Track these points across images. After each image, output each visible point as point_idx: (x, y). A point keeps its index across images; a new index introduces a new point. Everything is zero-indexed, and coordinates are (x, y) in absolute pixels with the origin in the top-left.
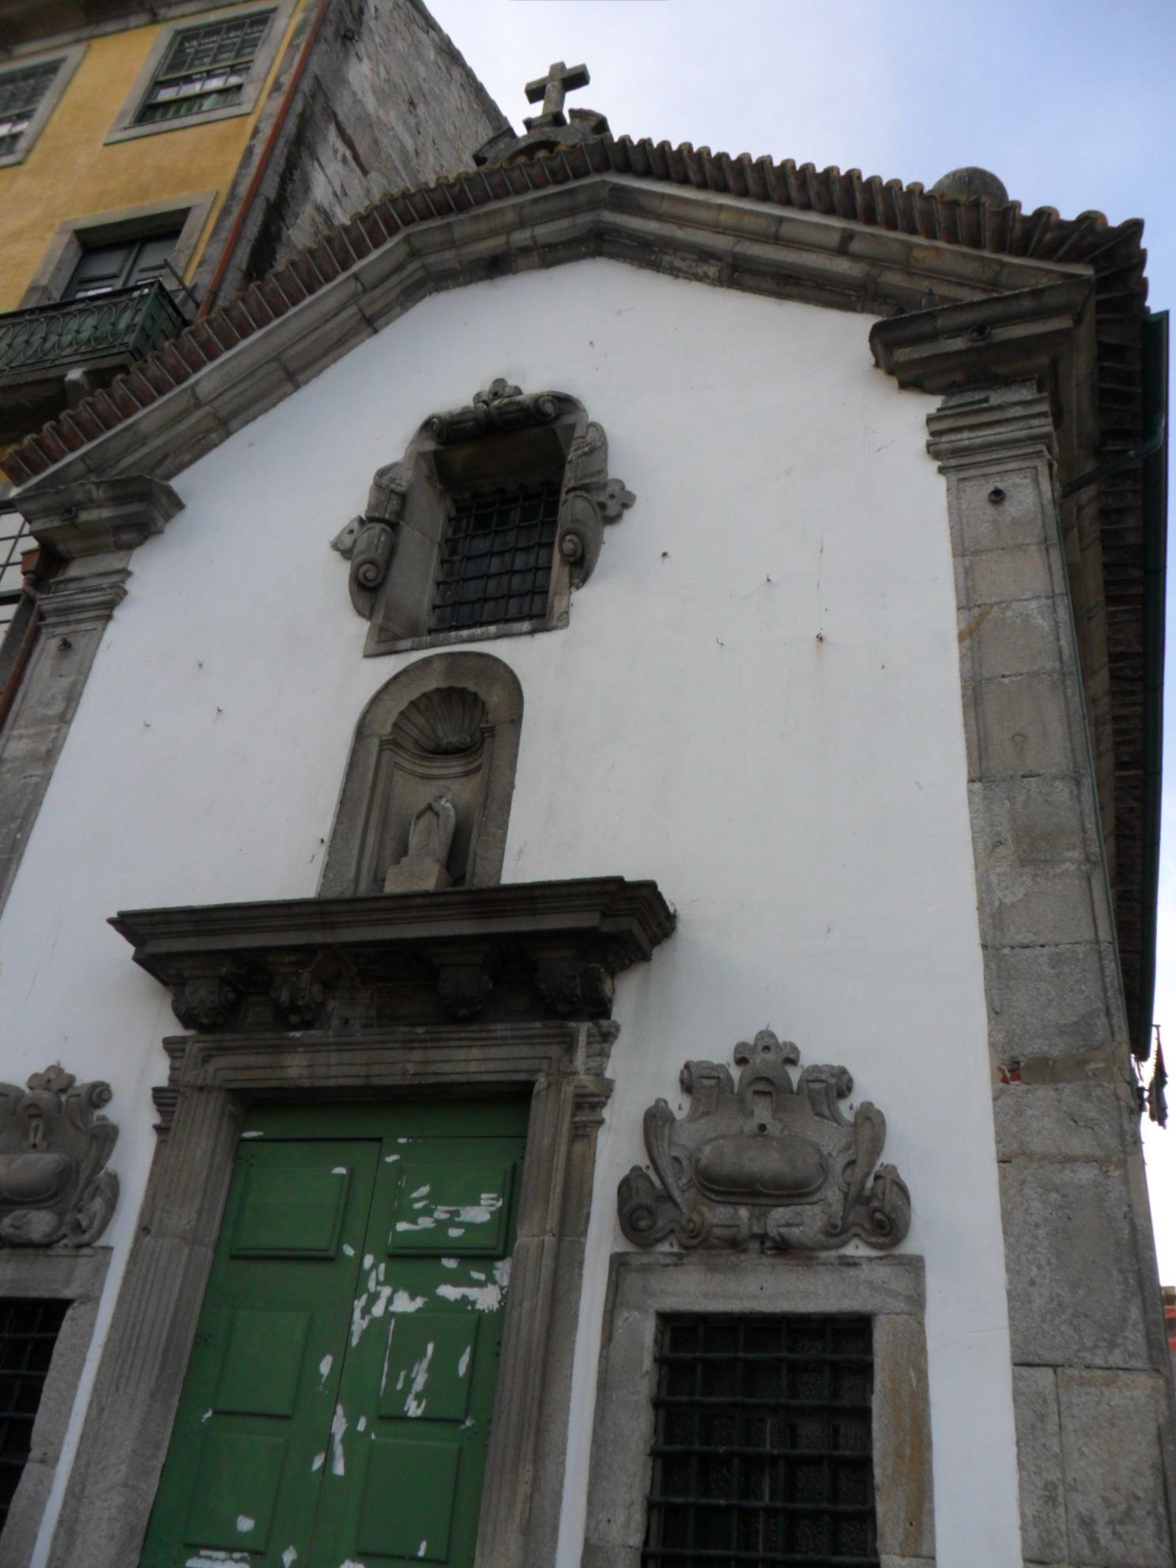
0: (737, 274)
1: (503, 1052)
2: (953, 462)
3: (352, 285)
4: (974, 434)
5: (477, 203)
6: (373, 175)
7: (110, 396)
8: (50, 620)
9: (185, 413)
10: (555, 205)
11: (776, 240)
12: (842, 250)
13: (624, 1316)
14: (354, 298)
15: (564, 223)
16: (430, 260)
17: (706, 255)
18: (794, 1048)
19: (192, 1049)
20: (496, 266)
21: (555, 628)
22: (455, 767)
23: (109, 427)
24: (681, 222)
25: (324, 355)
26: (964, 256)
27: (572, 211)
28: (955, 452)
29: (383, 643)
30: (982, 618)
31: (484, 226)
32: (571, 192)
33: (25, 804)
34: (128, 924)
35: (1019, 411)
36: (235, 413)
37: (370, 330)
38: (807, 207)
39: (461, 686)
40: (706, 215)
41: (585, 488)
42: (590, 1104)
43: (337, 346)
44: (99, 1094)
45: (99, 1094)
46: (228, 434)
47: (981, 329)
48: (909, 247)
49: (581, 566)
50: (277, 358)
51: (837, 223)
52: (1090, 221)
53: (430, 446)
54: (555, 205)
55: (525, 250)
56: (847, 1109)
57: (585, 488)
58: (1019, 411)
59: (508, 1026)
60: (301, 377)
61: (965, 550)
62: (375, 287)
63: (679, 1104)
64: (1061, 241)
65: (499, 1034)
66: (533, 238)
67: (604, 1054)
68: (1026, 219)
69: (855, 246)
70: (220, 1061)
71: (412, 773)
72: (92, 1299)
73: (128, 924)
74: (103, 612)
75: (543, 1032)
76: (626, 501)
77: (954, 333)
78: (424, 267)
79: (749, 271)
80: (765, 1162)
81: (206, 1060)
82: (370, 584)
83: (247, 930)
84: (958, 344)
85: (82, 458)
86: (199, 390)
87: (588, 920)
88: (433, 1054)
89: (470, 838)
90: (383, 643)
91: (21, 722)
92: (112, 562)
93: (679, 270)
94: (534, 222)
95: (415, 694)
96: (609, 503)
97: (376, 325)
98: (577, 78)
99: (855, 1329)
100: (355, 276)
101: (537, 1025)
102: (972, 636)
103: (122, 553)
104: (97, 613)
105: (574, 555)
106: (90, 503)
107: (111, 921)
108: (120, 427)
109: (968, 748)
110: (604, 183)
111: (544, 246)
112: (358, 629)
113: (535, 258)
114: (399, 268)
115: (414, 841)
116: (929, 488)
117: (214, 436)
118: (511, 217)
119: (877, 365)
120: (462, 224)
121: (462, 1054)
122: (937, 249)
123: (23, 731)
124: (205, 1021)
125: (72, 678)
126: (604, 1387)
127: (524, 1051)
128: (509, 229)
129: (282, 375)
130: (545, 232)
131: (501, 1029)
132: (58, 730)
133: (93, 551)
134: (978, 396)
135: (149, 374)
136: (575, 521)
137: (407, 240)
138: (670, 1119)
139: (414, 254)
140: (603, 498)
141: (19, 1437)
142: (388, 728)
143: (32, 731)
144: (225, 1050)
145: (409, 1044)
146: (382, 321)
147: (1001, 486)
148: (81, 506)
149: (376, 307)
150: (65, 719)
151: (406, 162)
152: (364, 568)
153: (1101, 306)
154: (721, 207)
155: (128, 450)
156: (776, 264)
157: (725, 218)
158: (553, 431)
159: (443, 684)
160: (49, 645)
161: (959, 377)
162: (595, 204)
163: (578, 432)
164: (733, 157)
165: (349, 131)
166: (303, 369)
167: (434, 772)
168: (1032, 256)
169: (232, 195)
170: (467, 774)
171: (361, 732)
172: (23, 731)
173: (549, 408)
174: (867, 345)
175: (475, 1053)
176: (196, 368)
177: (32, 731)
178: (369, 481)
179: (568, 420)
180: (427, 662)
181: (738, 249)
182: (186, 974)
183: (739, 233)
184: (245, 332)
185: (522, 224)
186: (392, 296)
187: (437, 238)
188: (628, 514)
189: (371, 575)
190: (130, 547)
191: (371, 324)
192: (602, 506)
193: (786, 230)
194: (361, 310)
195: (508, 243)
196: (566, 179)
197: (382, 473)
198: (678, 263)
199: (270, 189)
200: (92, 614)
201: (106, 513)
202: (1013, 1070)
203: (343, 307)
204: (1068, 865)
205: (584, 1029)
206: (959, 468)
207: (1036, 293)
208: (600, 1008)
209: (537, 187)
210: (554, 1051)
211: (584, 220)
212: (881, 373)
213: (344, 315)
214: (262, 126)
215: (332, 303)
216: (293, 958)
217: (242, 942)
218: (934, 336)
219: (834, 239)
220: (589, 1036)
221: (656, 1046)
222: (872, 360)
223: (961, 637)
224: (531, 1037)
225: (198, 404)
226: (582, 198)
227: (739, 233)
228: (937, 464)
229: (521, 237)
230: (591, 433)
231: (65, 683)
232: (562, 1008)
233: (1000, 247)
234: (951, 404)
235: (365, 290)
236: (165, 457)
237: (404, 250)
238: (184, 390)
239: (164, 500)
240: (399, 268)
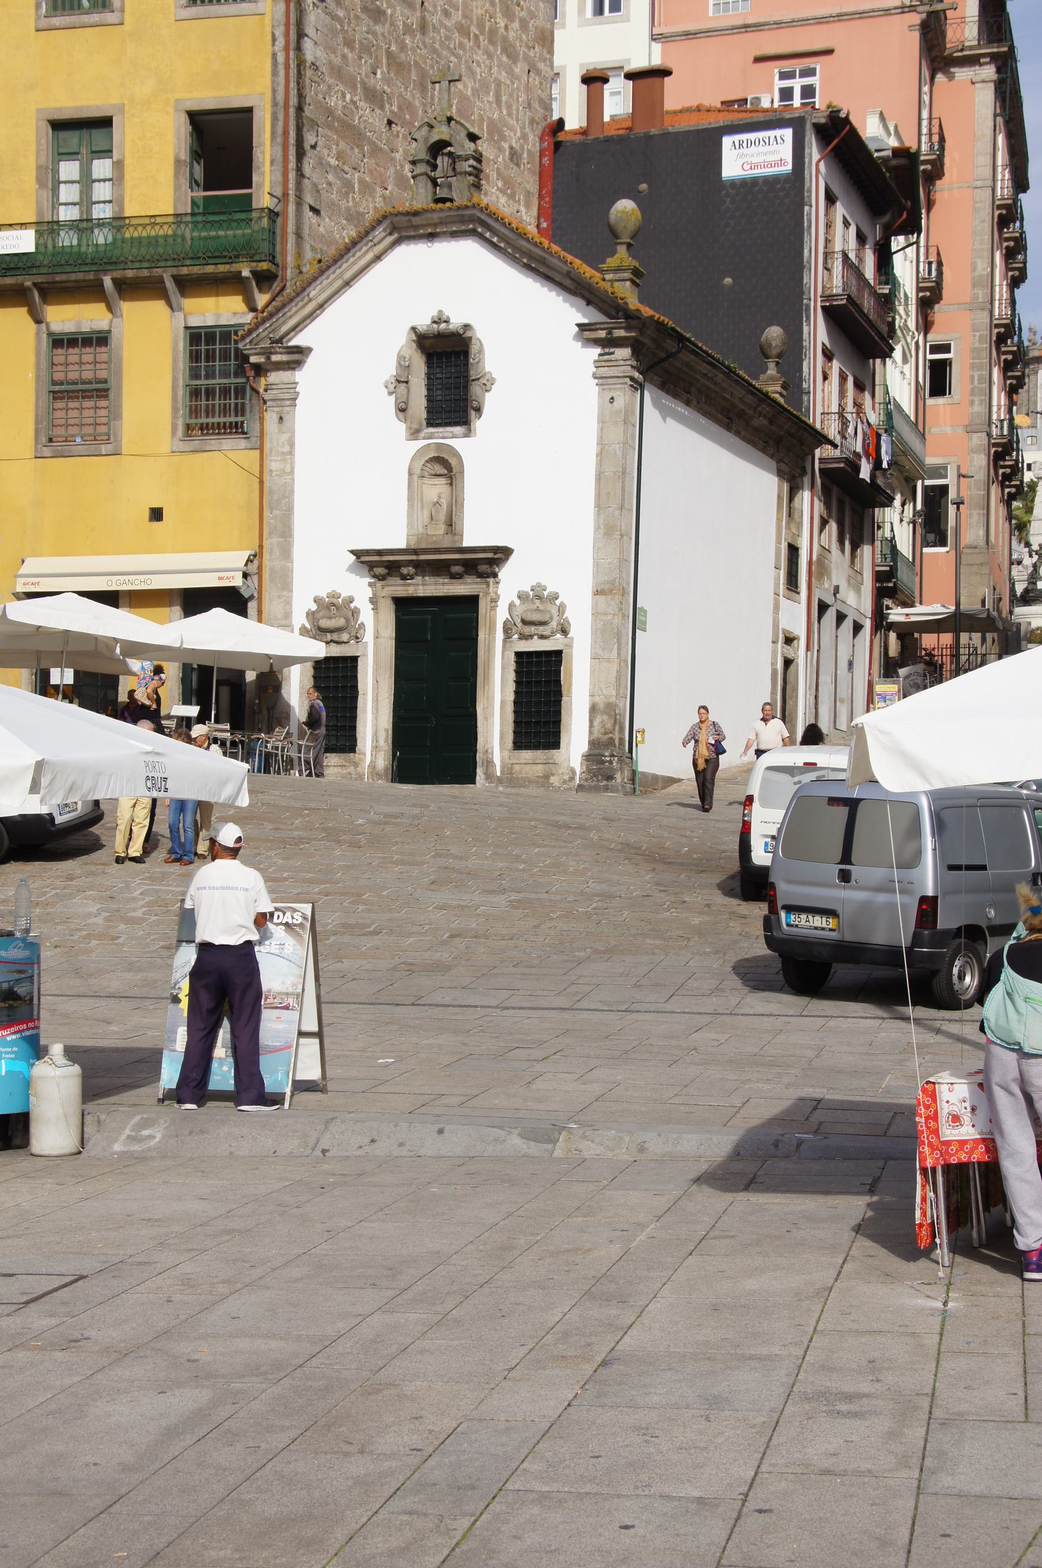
13: (507, 653)
20: (432, 237)
29: (414, 434)
32: (462, 216)
34: (353, 552)
35: (622, 363)
42: (495, 601)
44: (351, 600)
45: (351, 600)
56: (558, 602)
58: (622, 363)
63: (517, 602)
70: (387, 589)
72: (365, 655)
73: (353, 552)
76: (492, 381)
80: (536, 617)
87: (490, 555)
90: (414, 434)
99: (558, 653)
102: (600, 455)
112: (403, 426)
116: (591, 391)
120: (416, 220)
126: (503, 669)
127: (476, 586)
128: (436, 225)
137: (392, 223)
138: (515, 605)
141: (354, 688)
147: (614, 395)
150: (291, 453)
169: (275, 104)
171: (410, 474)
199: (293, 101)
202: (597, 593)
205: (491, 580)
208: (495, 575)
210: (484, 586)
214: (277, 33)
217: (391, 558)
221: (509, 585)
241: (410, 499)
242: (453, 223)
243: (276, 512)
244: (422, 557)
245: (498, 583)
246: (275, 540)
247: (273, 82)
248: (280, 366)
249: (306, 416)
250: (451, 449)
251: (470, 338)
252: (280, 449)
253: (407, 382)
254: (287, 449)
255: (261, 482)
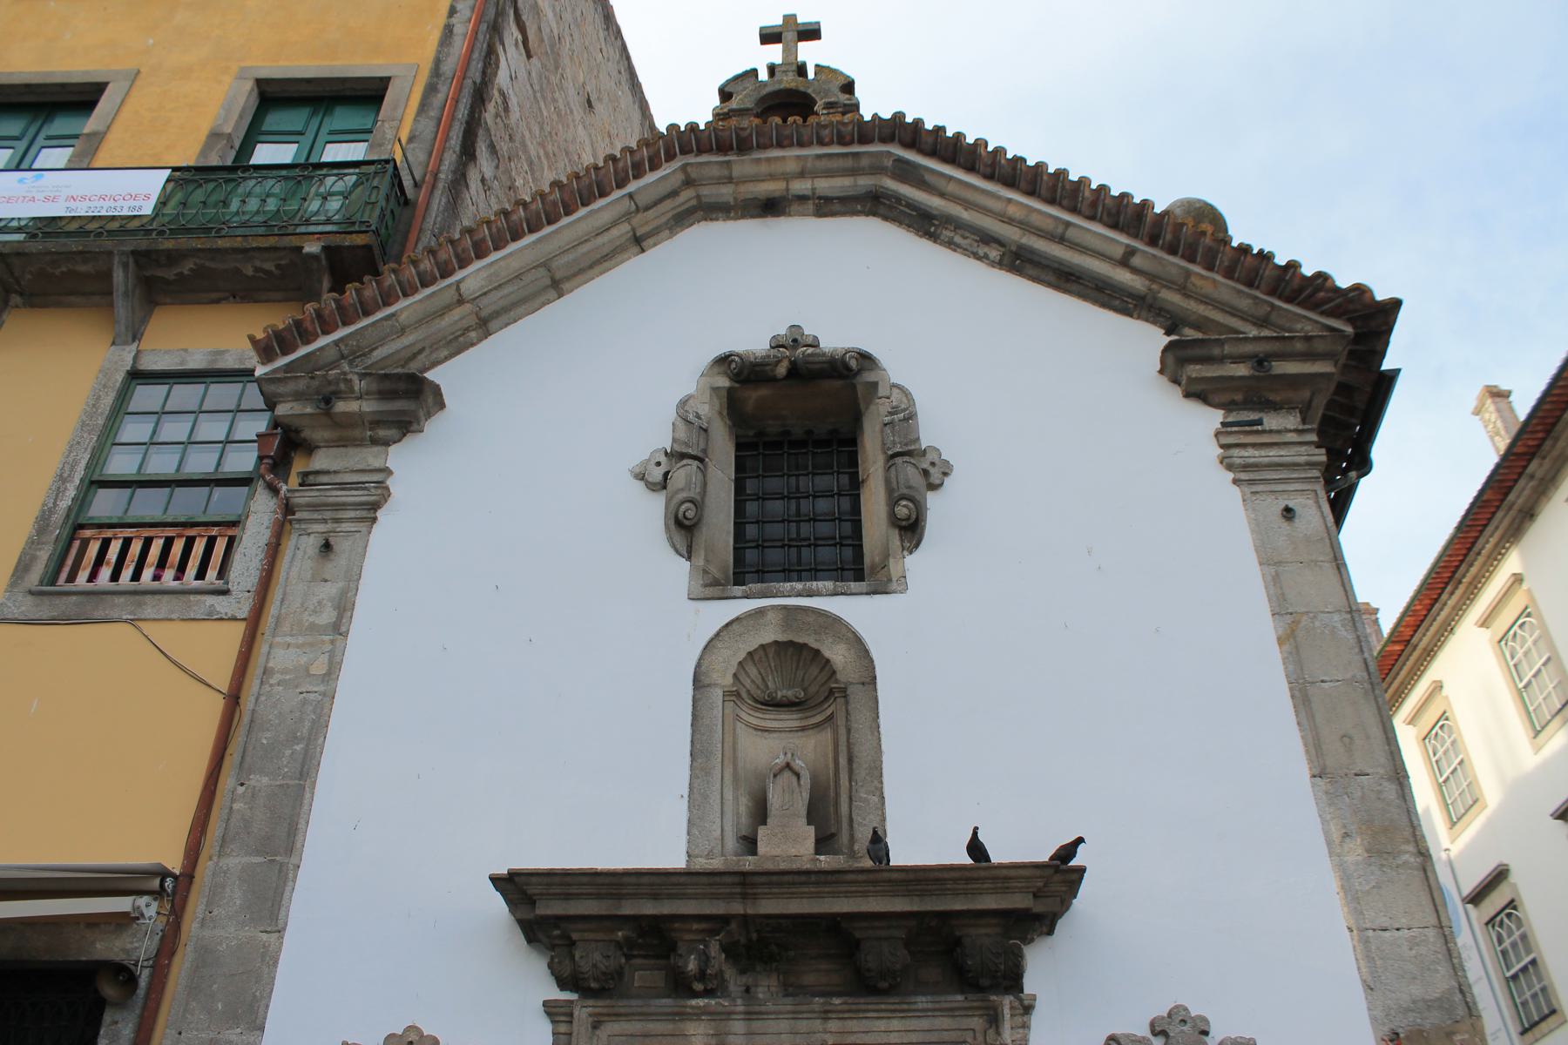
0: (1019, 261)
1: (924, 1024)
2: (1243, 476)
3: (627, 204)
4: (1257, 453)
5: (759, 147)
6: (534, 60)
7: (378, 283)
8: (298, 516)
9: (448, 308)
10: (840, 163)
11: (1061, 240)
12: (1124, 262)
14: (627, 216)
15: (846, 182)
16: (705, 191)
17: (987, 239)
18: (1205, 1020)
19: (582, 1013)
20: (771, 207)
21: (894, 592)
22: (789, 720)
23: (367, 314)
24: (968, 205)
25: (591, 267)
26: (1239, 292)
27: (853, 172)
28: (1246, 467)
29: (712, 587)
30: (1296, 622)
31: (764, 169)
33: (307, 724)
36: (496, 314)
37: (637, 249)
38: (1092, 218)
39: (801, 641)
40: (996, 206)
41: (909, 453)
43: (605, 260)
46: (487, 334)
47: (1260, 361)
48: (1188, 274)
49: (911, 529)
50: (545, 265)
51: (1124, 239)
52: (1360, 290)
53: (724, 382)
54: (840, 163)
55: (802, 199)
57: (909, 453)
59: (930, 998)
60: (566, 286)
61: (1270, 561)
62: (647, 208)
64: (1300, 290)
65: (920, 1006)
66: (813, 189)
67: (1026, 1026)
68: (1304, 278)
69: (1136, 261)
71: (748, 725)
74: (364, 514)
75: (966, 1004)
77: (1238, 359)
78: (698, 197)
79: (1031, 262)
81: (596, 1026)
82: (687, 523)
83: (655, 897)
84: (1242, 370)
85: (336, 343)
86: (463, 287)
88: (852, 1025)
89: (838, 802)
91: (286, 628)
92: (370, 457)
93: (958, 246)
94: (814, 174)
95: (753, 644)
96: (932, 470)
97: (644, 244)
98: (811, 33)
100: (631, 196)
101: (960, 998)
103: (376, 449)
104: (358, 514)
105: (908, 519)
106: (348, 394)
107: (496, 880)
108: (379, 315)
109: (1306, 745)
110: (889, 153)
111: (820, 198)
112: (678, 571)
113: (810, 206)
114: (674, 194)
115: (775, 799)
117: (473, 334)
118: (792, 167)
119: (1161, 372)
120: (742, 165)
121: (881, 1025)
122: (1214, 281)
123: (288, 639)
124: (593, 985)
125: (341, 585)
127: (946, 1022)
129: (548, 282)
130: (825, 186)
131: (922, 1001)
132: (332, 642)
133: (343, 443)
134: (1253, 416)
135: (422, 267)
136: (910, 487)
137: (684, 168)
139: (689, 183)
140: (925, 465)
142: (729, 680)
143: (301, 640)
144: (618, 1016)
145: (825, 1015)
146: (650, 241)
148: (338, 395)
149: (646, 229)
150: (339, 628)
151: (552, 46)
152: (683, 507)
153: (1351, 353)
154: (1010, 201)
155: (382, 341)
156: (1060, 262)
157: (1011, 210)
158: (854, 387)
159: (781, 638)
160: (301, 548)
161: (1239, 397)
162: (877, 170)
163: (882, 391)
164: (1031, 162)
165: (524, 18)
166: (568, 279)
167: (769, 724)
168: (1299, 304)
169: (436, 72)
170: (803, 729)
171: (700, 682)
172: (288, 639)
173: (853, 364)
174: (1159, 354)
175: (896, 1024)
176: (463, 264)
177: (301, 640)
178: (671, 414)
179: (869, 377)
180: (761, 612)
181: (1024, 241)
182: (575, 936)
183: (1025, 226)
184: (516, 237)
185: (802, 175)
186: (664, 219)
187: (715, 172)
188: (947, 481)
189: (690, 514)
190: (387, 443)
191: (639, 242)
192: (926, 473)
193: (1070, 233)
194: (634, 230)
195: (787, 189)
196: (851, 143)
197: (683, 403)
198: (958, 239)
200: (352, 514)
201: (368, 406)
203: (615, 223)
204: (1406, 857)
205: (1007, 1001)
206: (1251, 482)
207: (1308, 339)
208: (1013, 981)
209: (821, 143)
211: (865, 182)
212: (1164, 380)
213: (615, 232)
215: (606, 217)
216: (703, 926)
217: (649, 908)
218: (1221, 360)
219: (1118, 252)
220: (1012, 1008)
222: (1158, 367)
223: (1280, 641)
224: (952, 1009)
225: (461, 301)
226: (865, 162)
227: (1025, 226)
228: (1231, 476)
229: (801, 186)
230: (896, 393)
231: (331, 590)
232: (985, 982)
233: (1272, 292)
234: (1230, 419)
235: (638, 210)
236: (421, 351)
237: (681, 177)
238: (449, 286)
239: (430, 400)
240: (674, 194)
241: (698, 752)
242: (829, 174)
243: (260, 781)
244: (769, 906)
245: (1028, 1009)
246: (235, 861)
247: (439, 52)
248: (349, 433)
249: (392, 551)
250: (833, 624)
251: (875, 385)
252: (308, 618)
253: (701, 460)
254: (327, 616)
255: (233, 699)
